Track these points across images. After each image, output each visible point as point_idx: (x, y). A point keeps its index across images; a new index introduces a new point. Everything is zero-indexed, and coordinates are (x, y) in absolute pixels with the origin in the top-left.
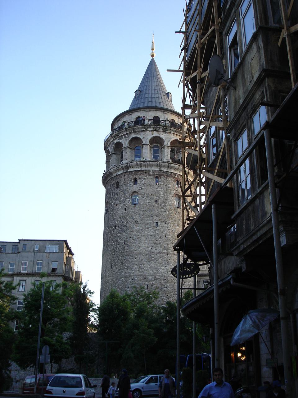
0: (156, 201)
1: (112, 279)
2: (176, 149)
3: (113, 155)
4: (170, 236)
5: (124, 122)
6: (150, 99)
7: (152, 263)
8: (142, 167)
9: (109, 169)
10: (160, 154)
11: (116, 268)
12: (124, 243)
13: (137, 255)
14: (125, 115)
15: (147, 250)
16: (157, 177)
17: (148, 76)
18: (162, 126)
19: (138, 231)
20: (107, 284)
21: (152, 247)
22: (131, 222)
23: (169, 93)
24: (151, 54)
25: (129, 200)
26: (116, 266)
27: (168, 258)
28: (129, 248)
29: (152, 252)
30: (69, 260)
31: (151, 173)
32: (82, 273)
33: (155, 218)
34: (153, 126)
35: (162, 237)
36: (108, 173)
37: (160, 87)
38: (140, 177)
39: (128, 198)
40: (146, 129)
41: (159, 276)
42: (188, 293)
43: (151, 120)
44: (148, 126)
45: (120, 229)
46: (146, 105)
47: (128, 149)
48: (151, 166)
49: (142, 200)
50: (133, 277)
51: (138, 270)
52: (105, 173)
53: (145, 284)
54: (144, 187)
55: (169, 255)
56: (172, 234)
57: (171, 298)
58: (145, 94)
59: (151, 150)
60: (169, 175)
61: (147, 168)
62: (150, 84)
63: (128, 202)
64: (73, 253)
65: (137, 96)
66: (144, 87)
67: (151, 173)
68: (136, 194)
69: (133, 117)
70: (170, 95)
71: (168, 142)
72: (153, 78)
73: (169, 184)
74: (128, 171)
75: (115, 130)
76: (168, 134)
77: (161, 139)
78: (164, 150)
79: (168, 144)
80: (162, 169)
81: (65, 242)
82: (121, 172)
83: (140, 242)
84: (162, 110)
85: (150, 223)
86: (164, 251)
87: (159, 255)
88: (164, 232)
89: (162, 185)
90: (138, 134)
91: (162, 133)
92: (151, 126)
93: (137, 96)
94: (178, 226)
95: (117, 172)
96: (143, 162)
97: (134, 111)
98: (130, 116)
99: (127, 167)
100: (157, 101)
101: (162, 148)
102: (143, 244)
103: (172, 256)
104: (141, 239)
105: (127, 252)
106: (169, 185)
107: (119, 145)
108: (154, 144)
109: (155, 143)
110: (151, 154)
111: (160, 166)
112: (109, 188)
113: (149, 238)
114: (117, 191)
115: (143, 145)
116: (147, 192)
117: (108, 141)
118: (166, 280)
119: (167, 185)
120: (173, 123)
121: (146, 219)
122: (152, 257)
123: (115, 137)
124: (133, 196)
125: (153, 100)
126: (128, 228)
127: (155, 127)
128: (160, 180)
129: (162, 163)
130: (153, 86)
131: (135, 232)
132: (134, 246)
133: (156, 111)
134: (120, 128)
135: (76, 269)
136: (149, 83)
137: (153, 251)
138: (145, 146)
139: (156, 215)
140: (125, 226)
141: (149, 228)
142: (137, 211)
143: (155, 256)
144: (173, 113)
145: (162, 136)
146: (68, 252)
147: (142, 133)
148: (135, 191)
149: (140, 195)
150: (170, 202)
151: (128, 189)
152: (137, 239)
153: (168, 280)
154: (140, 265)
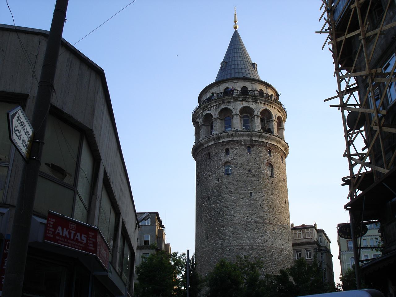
0: (249, 171)
1: (209, 250)
2: (266, 118)
3: (203, 126)
4: (265, 205)
5: (213, 93)
6: (237, 71)
8: (233, 137)
9: (200, 140)
10: (250, 124)
11: (212, 239)
12: (219, 214)
13: (233, 225)
14: (213, 87)
16: (249, 147)
17: (233, 47)
18: (252, 96)
19: (233, 201)
20: (203, 255)
22: (225, 192)
23: (254, 63)
24: (234, 26)
25: (221, 170)
26: (212, 237)
27: (264, 227)
28: (225, 218)
29: (248, 222)
30: (161, 233)
31: (243, 143)
32: (171, 246)
34: (243, 97)
35: (257, 207)
36: (198, 144)
37: (245, 58)
38: (232, 147)
39: (220, 168)
40: (235, 100)
41: (256, 246)
42: (301, 260)
43: (240, 90)
44: (237, 97)
45: (214, 200)
46: (233, 76)
47: (218, 120)
48: (242, 135)
50: (230, 248)
51: (235, 241)
52: (195, 145)
53: (243, 255)
56: (267, 203)
57: (270, 268)
58: (231, 65)
60: (260, 144)
61: (238, 138)
62: (236, 55)
64: (164, 225)
65: (223, 67)
66: (229, 59)
67: (243, 143)
68: (229, 164)
69: (222, 88)
70: (256, 65)
71: (258, 112)
72: (237, 50)
73: (261, 154)
74: (220, 141)
75: (204, 101)
76: (258, 104)
77: (251, 109)
78: (255, 120)
79: (258, 113)
80: (254, 139)
81: (157, 214)
82: (212, 143)
83: (236, 212)
84: (250, 81)
85: (245, 193)
86: (260, 221)
87: (255, 225)
88: (259, 202)
89: (254, 155)
90: (228, 105)
91: (251, 103)
92: (241, 97)
93: (223, 67)
94: (273, 195)
95: (208, 143)
96: (234, 132)
97: (222, 83)
98: (218, 87)
99: (219, 138)
100: (243, 72)
101: (252, 118)
102: (238, 214)
103: (268, 226)
104: (236, 209)
105: (222, 222)
106: (262, 155)
107: (208, 117)
108: (244, 115)
109: (245, 113)
110: (242, 124)
111: (251, 136)
112: (200, 159)
114: (209, 162)
115: (233, 115)
116: (240, 162)
117: (196, 113)
118: (263, 250)
119: (259, 154)
120: (261, 92)
122: (248, 227)
123: (204, 109)
124: (226, 166)
125: (240, 71)
126: (223, 198)
127: (245, 97)
128: (252, 149)
129: (252, 133)
130: (239, 57)
131: (230, 203)
132: (229, 216)
134: (209, 100)
135: (167, 242)
136: (235, 55)
137: (248, 221)
138: (235, 117)
139: (250, 185)
140: (219, 196)
141: (244, 198)
143: (251, 226)
144: (261, 83)
145: (251, 106)
146: (159, 225)
147: (232, 104)
149: (233, 165)
150: (263, 172)
151: (220, 160)
152: (232, 209)
153: (266, 250)
154: (236, 235)
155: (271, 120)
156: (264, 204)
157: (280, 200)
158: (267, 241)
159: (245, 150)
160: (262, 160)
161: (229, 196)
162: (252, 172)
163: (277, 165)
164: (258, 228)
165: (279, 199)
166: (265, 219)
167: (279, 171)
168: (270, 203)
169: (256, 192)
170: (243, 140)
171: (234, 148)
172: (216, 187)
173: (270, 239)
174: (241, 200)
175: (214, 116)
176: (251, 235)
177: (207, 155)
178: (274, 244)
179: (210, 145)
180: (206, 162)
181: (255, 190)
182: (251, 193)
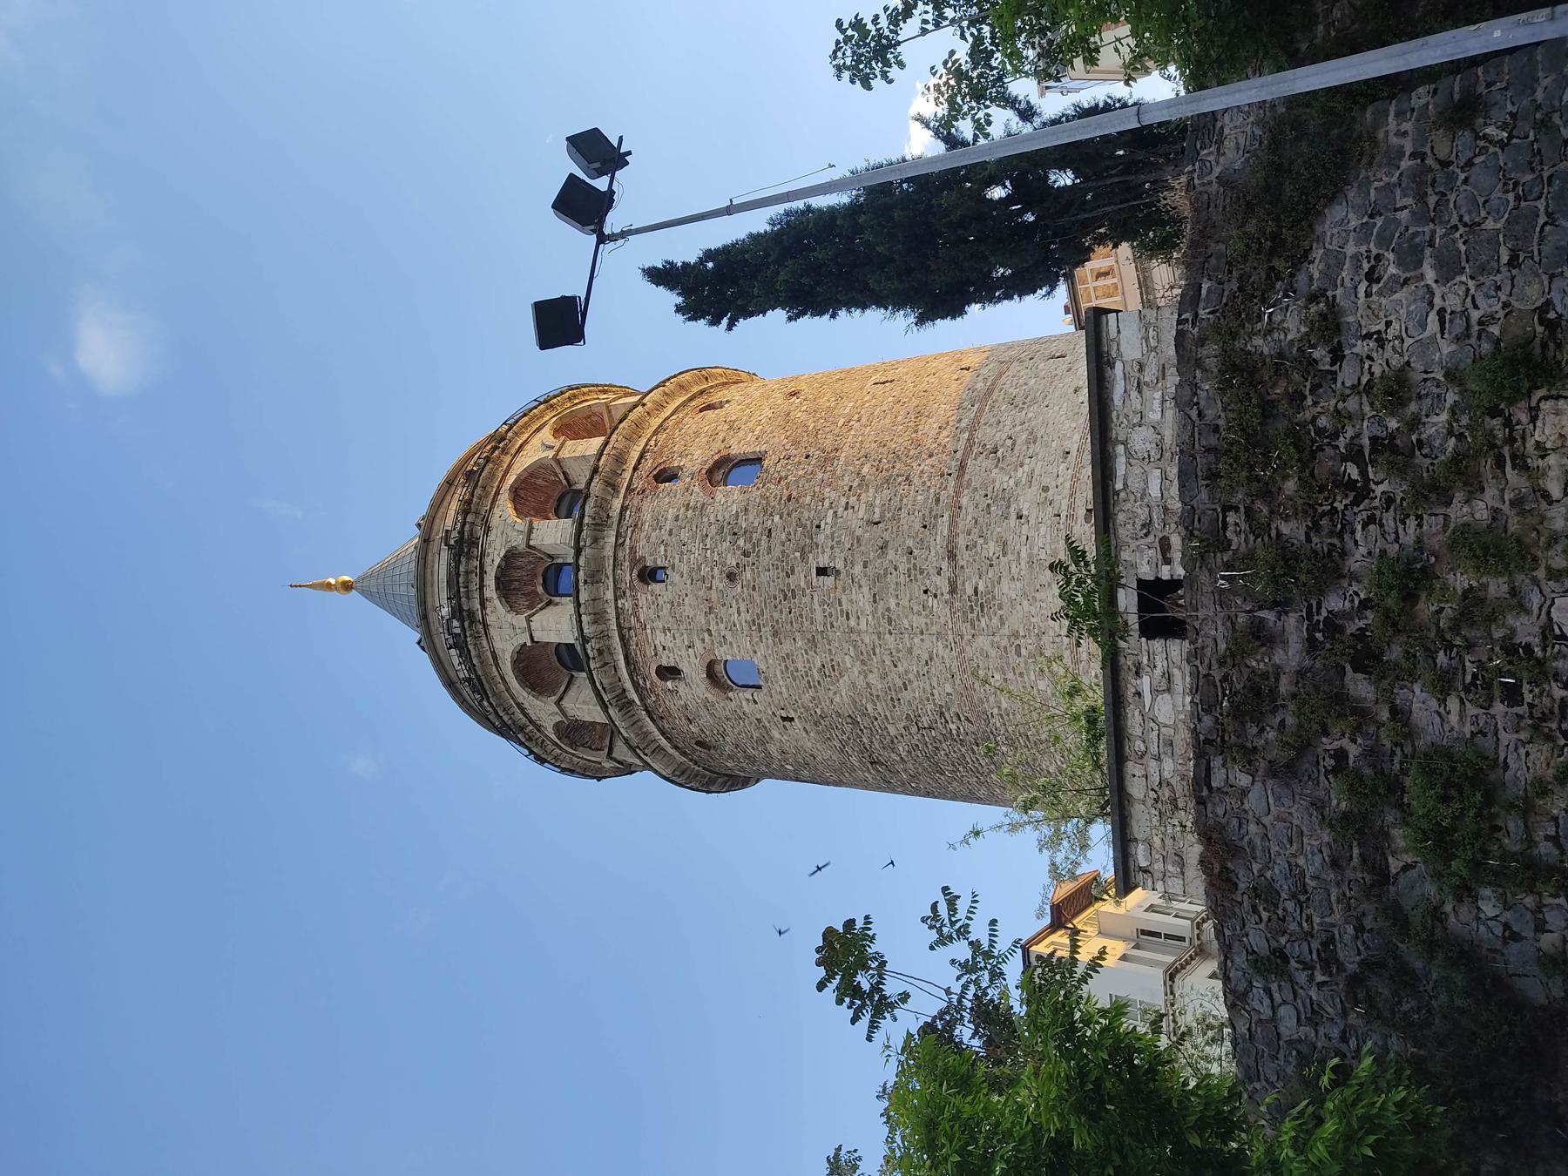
0: (731, 577)
7: (1005, 590)
15: (942, 620)
19: (863, 663)
21: (926, 592)
22: (831, 693)
25: (744, 703)
29: (953, 591)
33: (799, 580)
55: (964, 501)
59: (557, 604)
68: (719, 668)
76: (494, 531)
83: (910, 651)
85: (823, 603)
87: (966, 554)
88: (859, 532)
89: (669, 549)
91: (488, 560)
99: (625, 705)
102: (916, 640)
103: (969, 485)
104: (899, 651)
105: (967, 719)
108: (540, 589)
113: (888, 610)
121: (806, 624)
122: (976, 589)
137: (946, 589)
140: (855, 723)
141: (844, 608)
142: (780, 665)
143: (969, 578)
147: (498, 645)
151: (707, 704)
152: (900, 668)
154: (1019, 655)
158: (1045, 489)
161: (846, 677)
162: (734, 564)
164: (981, 541)
166: (938, 501)
170: (616, 600)
172: (818, 733)
173: (1036, 472)
174: (852, 622)
175: (558, 719)
176: (1013, 579)
177: (712, 751)
178: (1067, 445)
181: (807, 549)
182: (822, 571)
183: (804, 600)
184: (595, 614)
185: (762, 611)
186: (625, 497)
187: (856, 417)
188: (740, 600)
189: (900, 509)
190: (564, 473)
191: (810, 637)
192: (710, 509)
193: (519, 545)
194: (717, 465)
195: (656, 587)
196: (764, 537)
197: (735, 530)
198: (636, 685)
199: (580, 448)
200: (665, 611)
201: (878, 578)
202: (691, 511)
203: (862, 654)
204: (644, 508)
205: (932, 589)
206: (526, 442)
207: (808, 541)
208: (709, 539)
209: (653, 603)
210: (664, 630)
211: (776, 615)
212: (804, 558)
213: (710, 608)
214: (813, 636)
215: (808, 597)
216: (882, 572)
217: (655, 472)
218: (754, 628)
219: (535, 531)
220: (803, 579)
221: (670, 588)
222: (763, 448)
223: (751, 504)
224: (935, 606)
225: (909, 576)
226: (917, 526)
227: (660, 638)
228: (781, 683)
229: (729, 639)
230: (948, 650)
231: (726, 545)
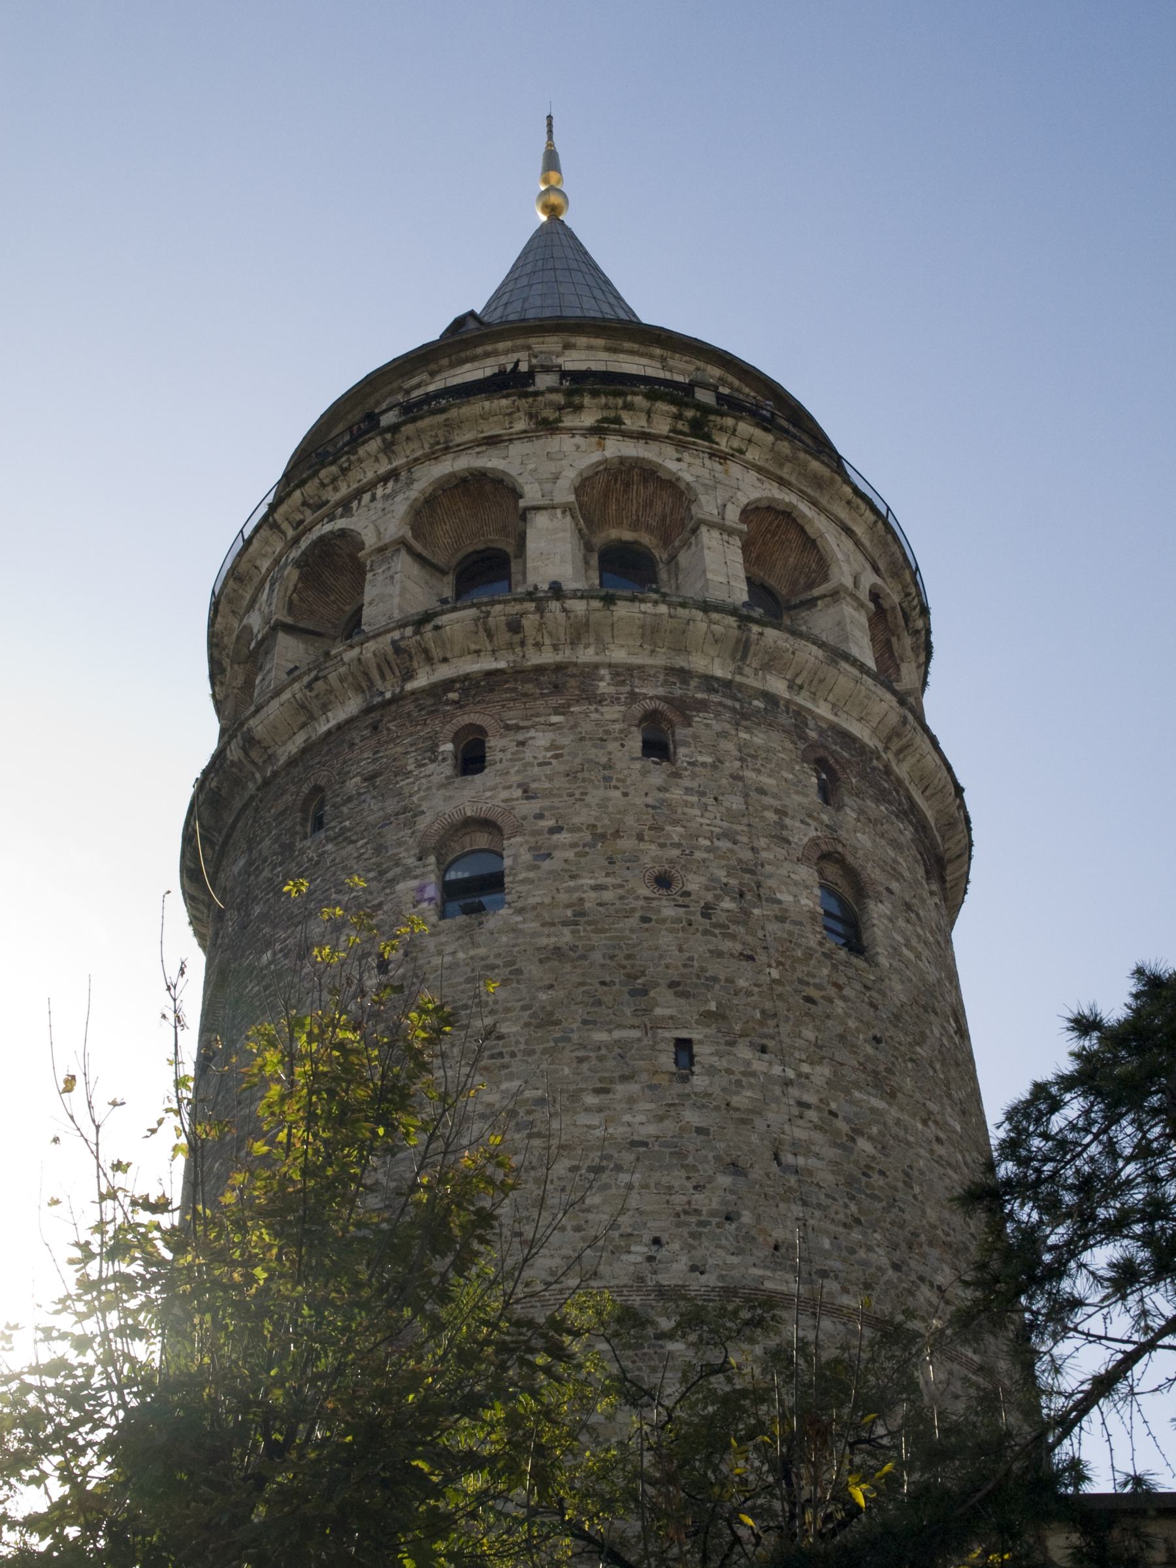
0: (663, 881)
3: (282, 638)
16: (651, 719)
19: (512, 1114)
25: (415, 883)
31: (604, 687)
33: (666, 1006)
39: (408, 874)
49: (531, 875)
54: (550, 779)
56: (836, 1145)
59: (587, 562)
63: (409, 898)
68: (482, 840)
73: (759, 771)
74: (409, 686)
77: (673, 487)
79: (722, 514)
80: (698, 663)
84: (658, 351)
85: (623, 1044)
88: (760, 1124)
91: (670, 450)
94: (876, 1086)
96: (531, 606)
113: (619, 1168)
116: (582, 817)
119: (749, 774)
133: (608, 349)
137: (665, 1279)
138: (541, 521)
139: (673, 985)
145: (672, 466)
147: (517, 449)
148: (469, 814)
149: (518, 839)
150: (786, 898)
151: (411, 814)
155: (816, 592)
156: (798, 1148)
157: (940, 1150)
159: (625, 733)
160: (771, 816)
163: (894, 886)
165: (939, 1140)
166: (824, 1274)
167: (919, 936)
168: (863, 1144)
169: (732, 1044)
170: (610, 666)
171: (522, 724)
174: (590, 1100)
175: (370, 540)
179: (323, 728)
180: (281, 864)
182: (684, 1046)
183: (628, 1012)
184: (587, 624)
185: (603, 931)
186: (788, 702)
187: (942, 1136)
188: (620, 891)
189: (805, 1204)
190: (811, 603)
191: (558, 1015)
192: (781, 852)
193: (701, 507)
194: (852, 874)
195: (635, 743)
196: (738, 947)
197: (748, 897)
198: (448, 685)
199: (857, 633)
200: (594, 751)
201: (681, 1155)
202: (775, 817)
203: (529, 1112)
204: (774, 735)
205: (662, 1254)
206: (858, 543)
207: (738, 1028)
208: (729, 845)
209: (607, 732)
210: (553, 746)
211: (597, 956)
212: (707, 1017)
213: (603, 836)
214: (558, 1023)
215: (636, 1022)
216: (690, 1160)
217: (832, 761)
218: (569, 913)
219: (725, 537)
220: (667, 1012)
221: (638, 765)
222: (883, 961)
223: (796, 929)
224: (632, 1258)
225: (686, 1212)
226: (779, 1234)
227: (541, 739)
228: (461, 955)
229: (546, 865)
230: (544, 1275)
231: (721, 874)
